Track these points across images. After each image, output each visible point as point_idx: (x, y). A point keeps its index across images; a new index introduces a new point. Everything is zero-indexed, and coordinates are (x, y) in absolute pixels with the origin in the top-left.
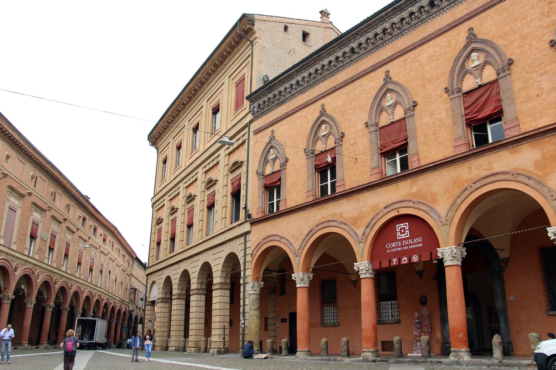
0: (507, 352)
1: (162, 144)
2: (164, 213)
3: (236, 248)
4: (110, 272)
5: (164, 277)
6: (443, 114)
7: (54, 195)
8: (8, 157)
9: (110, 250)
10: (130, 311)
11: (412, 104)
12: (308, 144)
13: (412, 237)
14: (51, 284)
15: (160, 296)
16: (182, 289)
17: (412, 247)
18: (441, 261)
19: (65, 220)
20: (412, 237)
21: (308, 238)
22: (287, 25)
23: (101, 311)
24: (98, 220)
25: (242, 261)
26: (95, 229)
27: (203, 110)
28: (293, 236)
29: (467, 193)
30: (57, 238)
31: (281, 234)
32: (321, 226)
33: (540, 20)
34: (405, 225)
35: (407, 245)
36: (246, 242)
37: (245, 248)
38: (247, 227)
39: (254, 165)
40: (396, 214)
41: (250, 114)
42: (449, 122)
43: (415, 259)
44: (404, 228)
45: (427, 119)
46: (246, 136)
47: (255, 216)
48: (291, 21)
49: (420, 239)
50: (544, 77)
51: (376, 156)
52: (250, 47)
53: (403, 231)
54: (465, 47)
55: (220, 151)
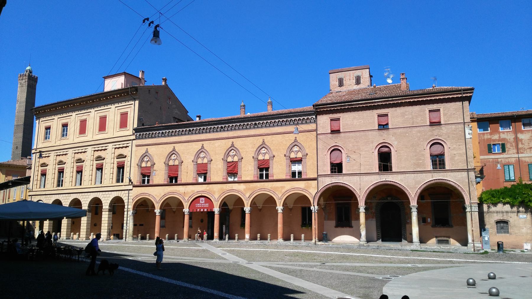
0: (230, 238)
3: (124, 195)
6: (220, 167)
11: (210, 160)
12: (166, 160)
13: (205, 203)
18: (214, 212)
20: (205, 203)
21: (163, 197)
25: (126, 201)
28: (156, 195)
29: (224, 193)
31: (150, 194)
32: (170, 194)
34: (203, 199)
38: (131, 187)
39: (135, 161)
42: (222, 170)
43: (205, 210)
45: (215, 166)
46: (130, 144)
47: (135, 183)
49: (208, 204)
50: (250, 166)
51: (195, 174)
53: (202, 201)
54: (230, 147)
55: (109, 144)
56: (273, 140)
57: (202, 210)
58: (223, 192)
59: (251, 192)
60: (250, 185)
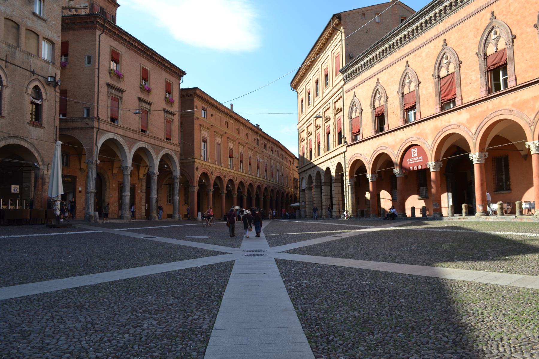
1: (300, 89)
2: (304, 135)
4: (278, 170)
5: (308, 175)
7: (238, 129)
8: (212, 115)
9: (276, 157)
10: (294, 194)
13: (418, 156)
14: (244, 182)
15: (307, 186)
16: (327, 179)
17: (418, 161)
18: (429, 169)
19: (247, 143)
22: (364, 13)
23: (275, 196)
24: (266, 139)
25: (344, 168)
26: (265, 146)
27: (320, 70)
28: (366, 154)
30: (244, 155)
33: (473, 39)
34: (414, 150)
35: (416, 160)
36: (345, 156)
37: (345, 160)
38: (344, 148)
40: (411, 144)
41: (342, 80)
42: (434, 94)
43: (420, 168)
44: (414, 151)
46: (342, 94)
48: (366, 9)
49: (421, 157)
50: (473, 73)
52: (340, 34)
56: (509, 5)
57: (415, 168)
58: (437, 133)
59: (478, 123)
60: (476, 110)
